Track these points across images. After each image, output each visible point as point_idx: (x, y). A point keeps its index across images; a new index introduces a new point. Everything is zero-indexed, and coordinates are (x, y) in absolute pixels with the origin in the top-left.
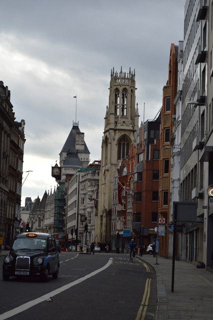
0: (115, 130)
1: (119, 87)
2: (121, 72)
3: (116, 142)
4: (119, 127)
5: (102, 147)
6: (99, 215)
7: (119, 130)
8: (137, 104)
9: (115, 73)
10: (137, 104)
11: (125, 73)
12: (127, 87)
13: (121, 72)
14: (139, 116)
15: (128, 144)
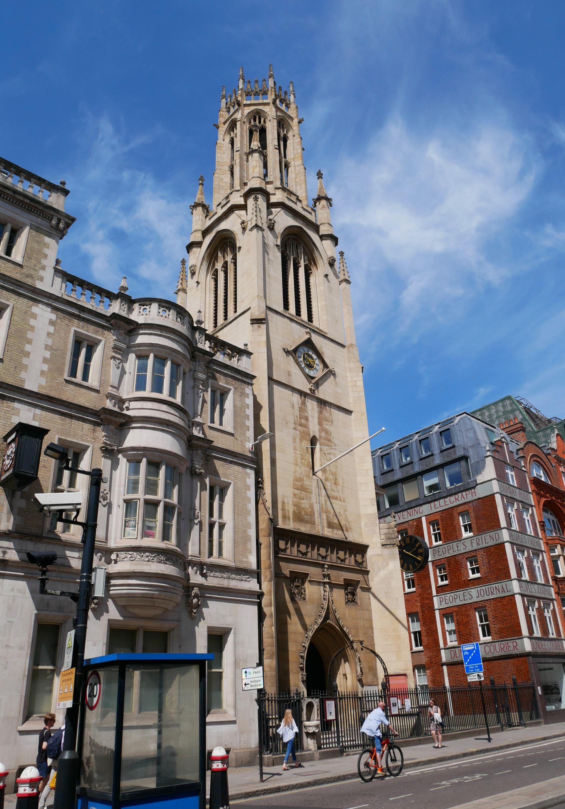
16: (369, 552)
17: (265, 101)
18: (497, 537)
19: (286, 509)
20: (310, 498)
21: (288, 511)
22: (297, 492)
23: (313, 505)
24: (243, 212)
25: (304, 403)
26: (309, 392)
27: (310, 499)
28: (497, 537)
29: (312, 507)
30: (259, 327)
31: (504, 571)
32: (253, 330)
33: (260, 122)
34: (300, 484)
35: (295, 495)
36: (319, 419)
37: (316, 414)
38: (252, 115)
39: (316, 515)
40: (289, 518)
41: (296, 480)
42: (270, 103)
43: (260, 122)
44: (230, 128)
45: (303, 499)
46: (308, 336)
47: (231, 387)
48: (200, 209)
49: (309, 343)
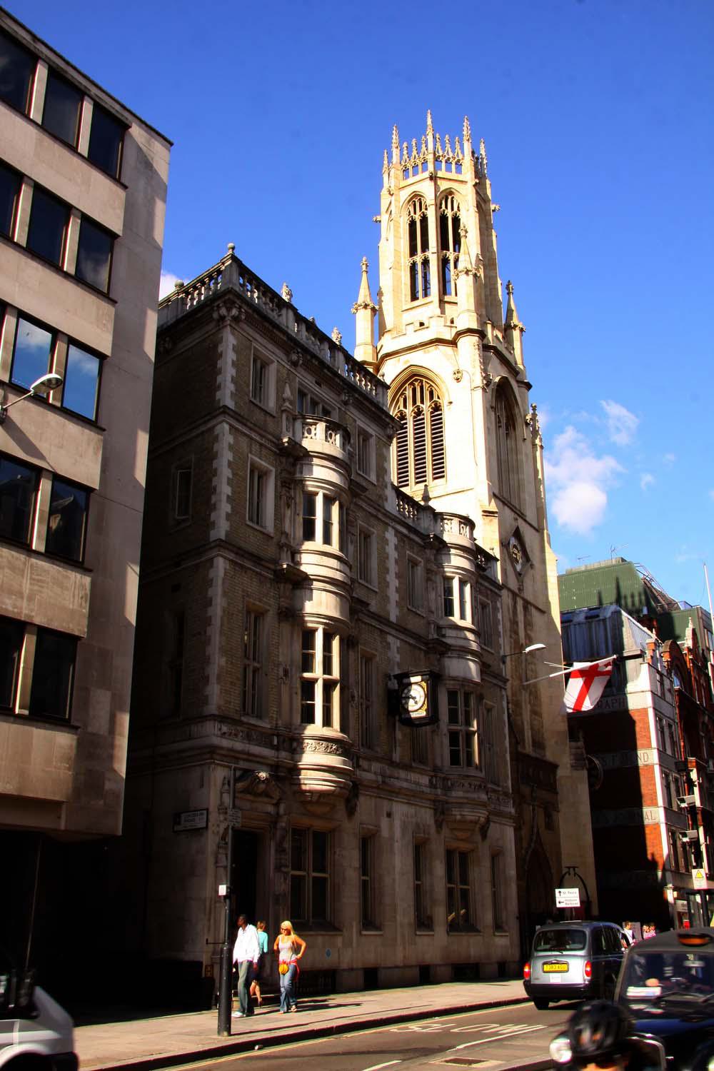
16: (560, 773)
17: (460, 177)
18: (646, 757)
24: (448, 350)
26: (517, 591)
28: (646, 757)
30: (491, 521)
31: (651, 796)
32: (485, 524)
33: (452, 209)
37: (523, 618)
38: (444, 194)
42: (466, 182)
43: (452, 209)
44: (409, 201)
46: (514, 524)
47: (489, 602)
48: (369, 311)
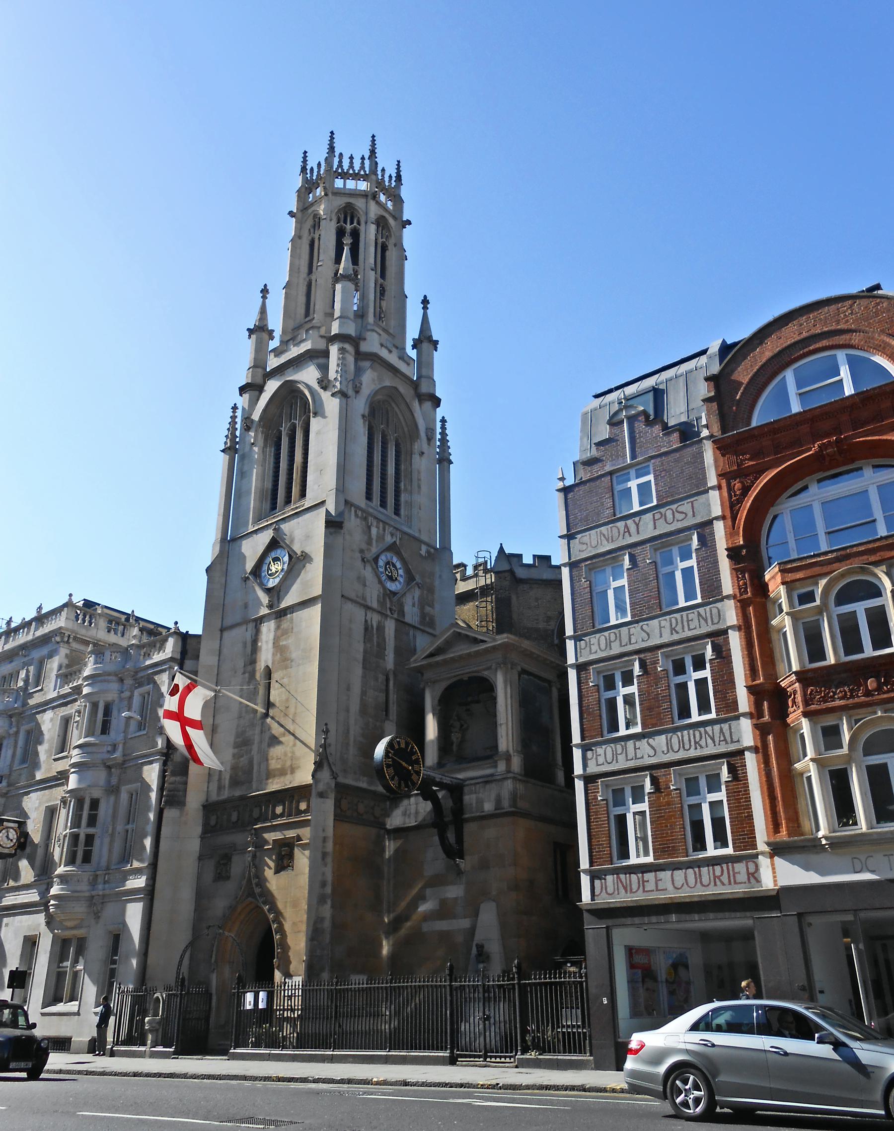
0: (360, 356)
1: (360, 203)
2: (373, 152)
3: (360, 405)
4: (372, 344)
5: (231, 449)
6: (194, 799)
7: (374, 358)
8: (425, 302)
9: (337, 154)
10: (425, 302)
11: (383, 170)
12: (391, 222)
13: (373, 152)
14: (436, 342)
15: (397, 445)
19: (223, 777)
20: (251, 750)
21: (225, 778)
22: (236, 750)
23: (253, 758)
25: (257, 631)
27: (250, 753)
29: (251, 762)
34: (241, 739)
35: (234, 755)
36: (274, 639)
37: (271, 636)
39: (255, 770)
40: (224, 786)
41: (238, 736)
45: (242, 756)
49: (274, 544)
